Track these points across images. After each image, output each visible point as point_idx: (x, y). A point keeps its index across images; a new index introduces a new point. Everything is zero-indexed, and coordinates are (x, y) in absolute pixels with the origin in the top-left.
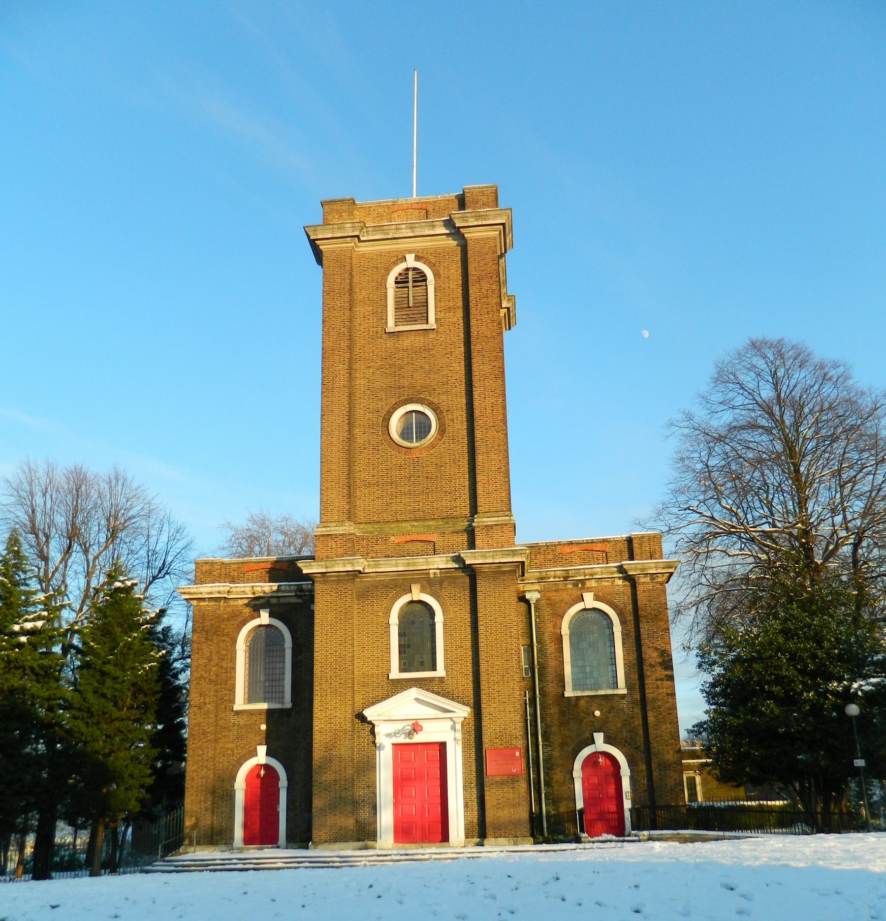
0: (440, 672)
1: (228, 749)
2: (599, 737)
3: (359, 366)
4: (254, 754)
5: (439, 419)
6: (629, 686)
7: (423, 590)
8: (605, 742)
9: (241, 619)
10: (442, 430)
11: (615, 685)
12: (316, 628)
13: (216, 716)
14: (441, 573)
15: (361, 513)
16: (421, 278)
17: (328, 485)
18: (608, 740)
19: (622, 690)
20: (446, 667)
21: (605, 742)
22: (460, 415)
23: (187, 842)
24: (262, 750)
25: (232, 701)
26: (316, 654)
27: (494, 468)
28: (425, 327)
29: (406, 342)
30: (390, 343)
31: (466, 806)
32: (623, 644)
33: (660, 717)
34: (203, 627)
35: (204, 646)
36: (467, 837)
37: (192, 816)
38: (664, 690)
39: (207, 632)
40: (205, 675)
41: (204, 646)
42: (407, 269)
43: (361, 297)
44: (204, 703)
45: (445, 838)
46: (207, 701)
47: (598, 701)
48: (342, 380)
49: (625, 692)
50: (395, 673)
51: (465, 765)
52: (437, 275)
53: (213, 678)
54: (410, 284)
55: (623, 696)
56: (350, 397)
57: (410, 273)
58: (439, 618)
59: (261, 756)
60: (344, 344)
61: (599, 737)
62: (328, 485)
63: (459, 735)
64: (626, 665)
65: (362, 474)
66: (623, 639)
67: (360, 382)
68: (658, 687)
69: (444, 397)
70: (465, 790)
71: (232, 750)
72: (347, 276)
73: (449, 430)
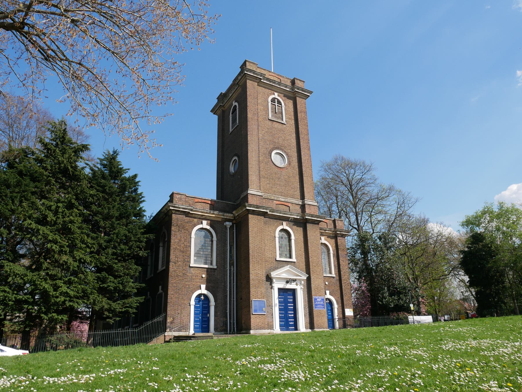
0: (294, 259)
1: (186, 285)
6: (335, 274)
7: (287, 225)
11: (331, 273)
12: (250, 233)
16: (279, 102)
18: (331, 294)
20: (296, 258)
23: (168, 330)
24: (203, 286)
26: (250, 245)
31: (305, 316)
34: (177, 224)
35: (178, 233)
37: (171, 317)
39: (179, 226)
40: (178, 248)
41: (178, 233)
44: (177, 261)
45: (296, 329)
46: (179, 260)
49: (334, 276)
50: (278, 258)
58: (293, 237)
59: (203, 290)
69: (289, 151)
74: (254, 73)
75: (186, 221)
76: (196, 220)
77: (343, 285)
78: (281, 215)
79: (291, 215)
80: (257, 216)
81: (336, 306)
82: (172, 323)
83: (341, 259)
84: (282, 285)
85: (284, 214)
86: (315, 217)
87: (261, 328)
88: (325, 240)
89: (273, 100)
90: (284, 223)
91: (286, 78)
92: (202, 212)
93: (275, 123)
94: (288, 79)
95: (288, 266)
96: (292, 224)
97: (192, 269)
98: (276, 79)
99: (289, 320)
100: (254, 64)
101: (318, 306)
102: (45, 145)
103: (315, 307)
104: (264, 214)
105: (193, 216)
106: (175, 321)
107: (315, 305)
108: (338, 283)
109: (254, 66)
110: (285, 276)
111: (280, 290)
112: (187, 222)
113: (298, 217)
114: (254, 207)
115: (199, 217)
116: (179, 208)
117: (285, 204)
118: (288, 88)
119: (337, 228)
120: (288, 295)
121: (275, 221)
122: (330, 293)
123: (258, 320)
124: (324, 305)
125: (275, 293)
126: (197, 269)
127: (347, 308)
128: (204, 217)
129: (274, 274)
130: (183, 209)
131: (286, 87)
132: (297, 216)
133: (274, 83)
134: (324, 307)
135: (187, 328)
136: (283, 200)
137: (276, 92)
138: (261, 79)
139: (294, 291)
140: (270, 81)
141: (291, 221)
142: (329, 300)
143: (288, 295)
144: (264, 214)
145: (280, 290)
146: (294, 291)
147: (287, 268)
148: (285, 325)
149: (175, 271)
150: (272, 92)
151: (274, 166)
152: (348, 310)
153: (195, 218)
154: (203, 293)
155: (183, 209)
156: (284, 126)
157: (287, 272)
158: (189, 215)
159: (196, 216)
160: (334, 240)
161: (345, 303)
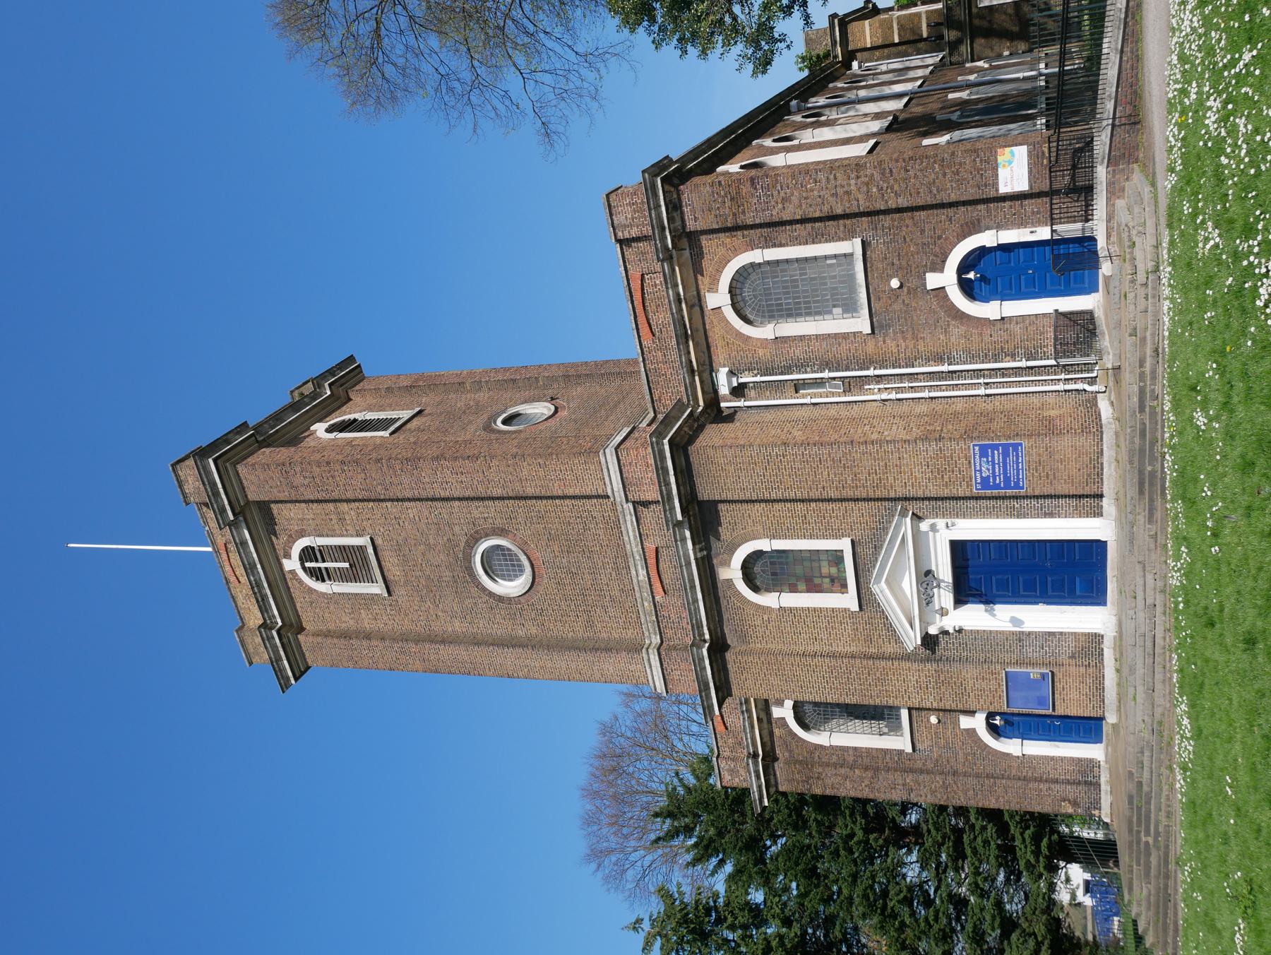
0: (844, 545)
2: (933, 281)
3: (437, 627)
4: (972, 732)
5: (487, 535)
6: (849, 236)
7: (727, 563)
8: (942, 270)
9: (789, 739)
10: (501, 532)
13: (922, 772)
14: (700, 543)
15: (630, 633)
16: (308, 554)
17: (598, 675)
18: (939, 267)
19: (853, 246)
21: (942, 270)
22: (477, 510)
25: (900, 752)
27: (541, 473)
28: (370, 550)
29: (394, 572)
30: (399, 592)
31: (1051, 515)
32: (781, 245)
33: (896, 187)
36: (1100, 514)
38: (853, 182)
39: (809, 778)
41: (829, 782)
42: (304, 568)
43: (352, 622)
47: (874, 282)
48: (462, 653)
49: (858, 242)
51: (984, 516)
52: (302, 534)
53: (869, 774)
54: (322, 565)
55: (865, 245)
56: (478, 644)
57: (308, 565)
58: (764, 545)
60: (413, 648)
61: (933, 281)
62: (598, 675)
63: (941, 523)
64: (815, 239)
65: (575, 629)
66: (774, 246)
67: (458, 626)
68: (848, 193)
69: (457, 529)
70: (1025, 516)
71: (966, 755)
72: (329, 640)
73: (499, 522)
74: (279, 659)
75: (786, 754)
76: (777, 732)
77: (892, 204)
78: (700, 596)
79: (688, 564)
80: (732, 676)
81: (987, 239)
82: (1075, 804)
83: (776, 214)
84: (945, 597)
85: (693, 587)
86: (668, 484)
87: (1100, 679)
88: (713, 288)
89: (318, 575)
90: (723, 574)
91: (206, 523)
92: (752, 727)
93: (390, 577)
94: (204, 516)
95: (875, 589)
96: (715, 544)
97: (918, 746)
98: (235, 558)
99: (1069, 572)
100: (242, 642)
101: (1012, 472)
102: (672, 834)
103: (1017, 486)
104: (719, 648)
105: (767, 739)
106: (1071, 797)
107: (1007, 486)
108: (887, 221)
109: (248, 640)
110: (909, 583)
111: (961, 598)
112: (790, 751)
113: (688, 534)
114: (709, 697)
115: (765, 725)
116: (760, 787)
117: (652, 561)
118: (241, 535)
119: (647, 230)
120: (980, 573)
121: (724, 603)
122: (933, 270)
123: (1074, 695)
124: (1006, 447)
125: (974, 617)
126: (915, 724)
127: (997, 190)
128: (763, 715)
129: (912, 639)
130: (758, 777)
131: (243, 543)
132: (684, 539)
133: (259, 585)
134: (1016, 447)
135: (1089, 766)
136: (642, 573)
137: (281, 565)
138: (278, 632)
139: (959, 549)
140: (264, 598)
141: (708, 548)
142: (963, 267)
143: (980, 573)
144: (719, 648)
145: (961, 598)
146: (959, 549)
147: (880, 589)
148: (1093, 593)
149: (933, 792)
150: (288, 576)
151: (539, 588)
152: (1002, 173)
153: (771, 734)
154: (984, 723)
155: (758, 777)
156: (379, 541)
157: (893, 583)
158: (768, 748)
159: (765, 732)
160: (704, 240)
161: (971, 193)
